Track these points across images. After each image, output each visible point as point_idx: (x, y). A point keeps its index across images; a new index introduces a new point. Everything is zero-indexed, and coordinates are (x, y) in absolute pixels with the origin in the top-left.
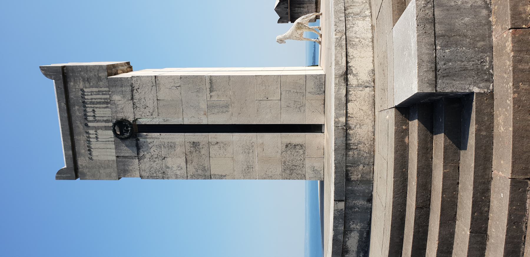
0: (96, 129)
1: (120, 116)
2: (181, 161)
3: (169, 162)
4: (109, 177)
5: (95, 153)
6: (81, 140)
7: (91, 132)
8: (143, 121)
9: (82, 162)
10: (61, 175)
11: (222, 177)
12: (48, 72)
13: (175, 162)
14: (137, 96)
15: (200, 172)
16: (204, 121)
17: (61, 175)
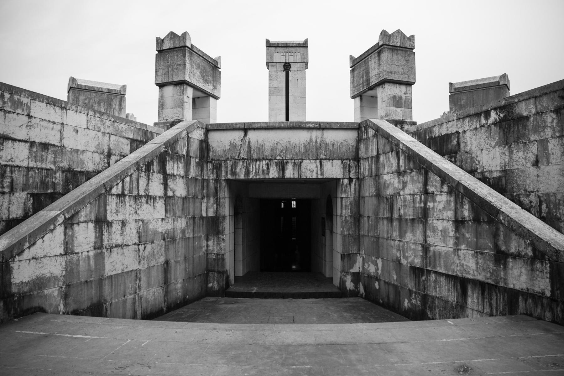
0: (286, 56)
1: (292, 66)
2: (275, 86)
3: (275, 82)
4: (267, 59)
5: (276, 54)
6: (282, 50)
7: (284, 54)
8: (290, 74)
9: (273, 49)
10: (268, 42)
11: (270, 100)
12: (306, 42)
13: (275, 84)
14: (299, 72)
15: (271, 92)
16: (290, 94)
17: (268, 42)
